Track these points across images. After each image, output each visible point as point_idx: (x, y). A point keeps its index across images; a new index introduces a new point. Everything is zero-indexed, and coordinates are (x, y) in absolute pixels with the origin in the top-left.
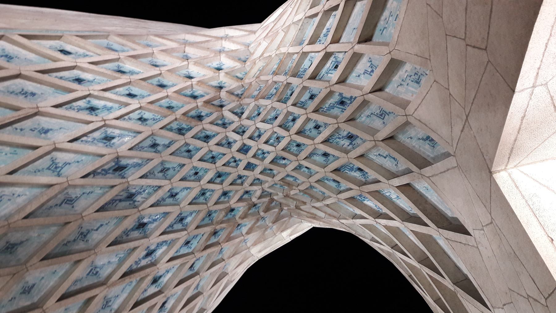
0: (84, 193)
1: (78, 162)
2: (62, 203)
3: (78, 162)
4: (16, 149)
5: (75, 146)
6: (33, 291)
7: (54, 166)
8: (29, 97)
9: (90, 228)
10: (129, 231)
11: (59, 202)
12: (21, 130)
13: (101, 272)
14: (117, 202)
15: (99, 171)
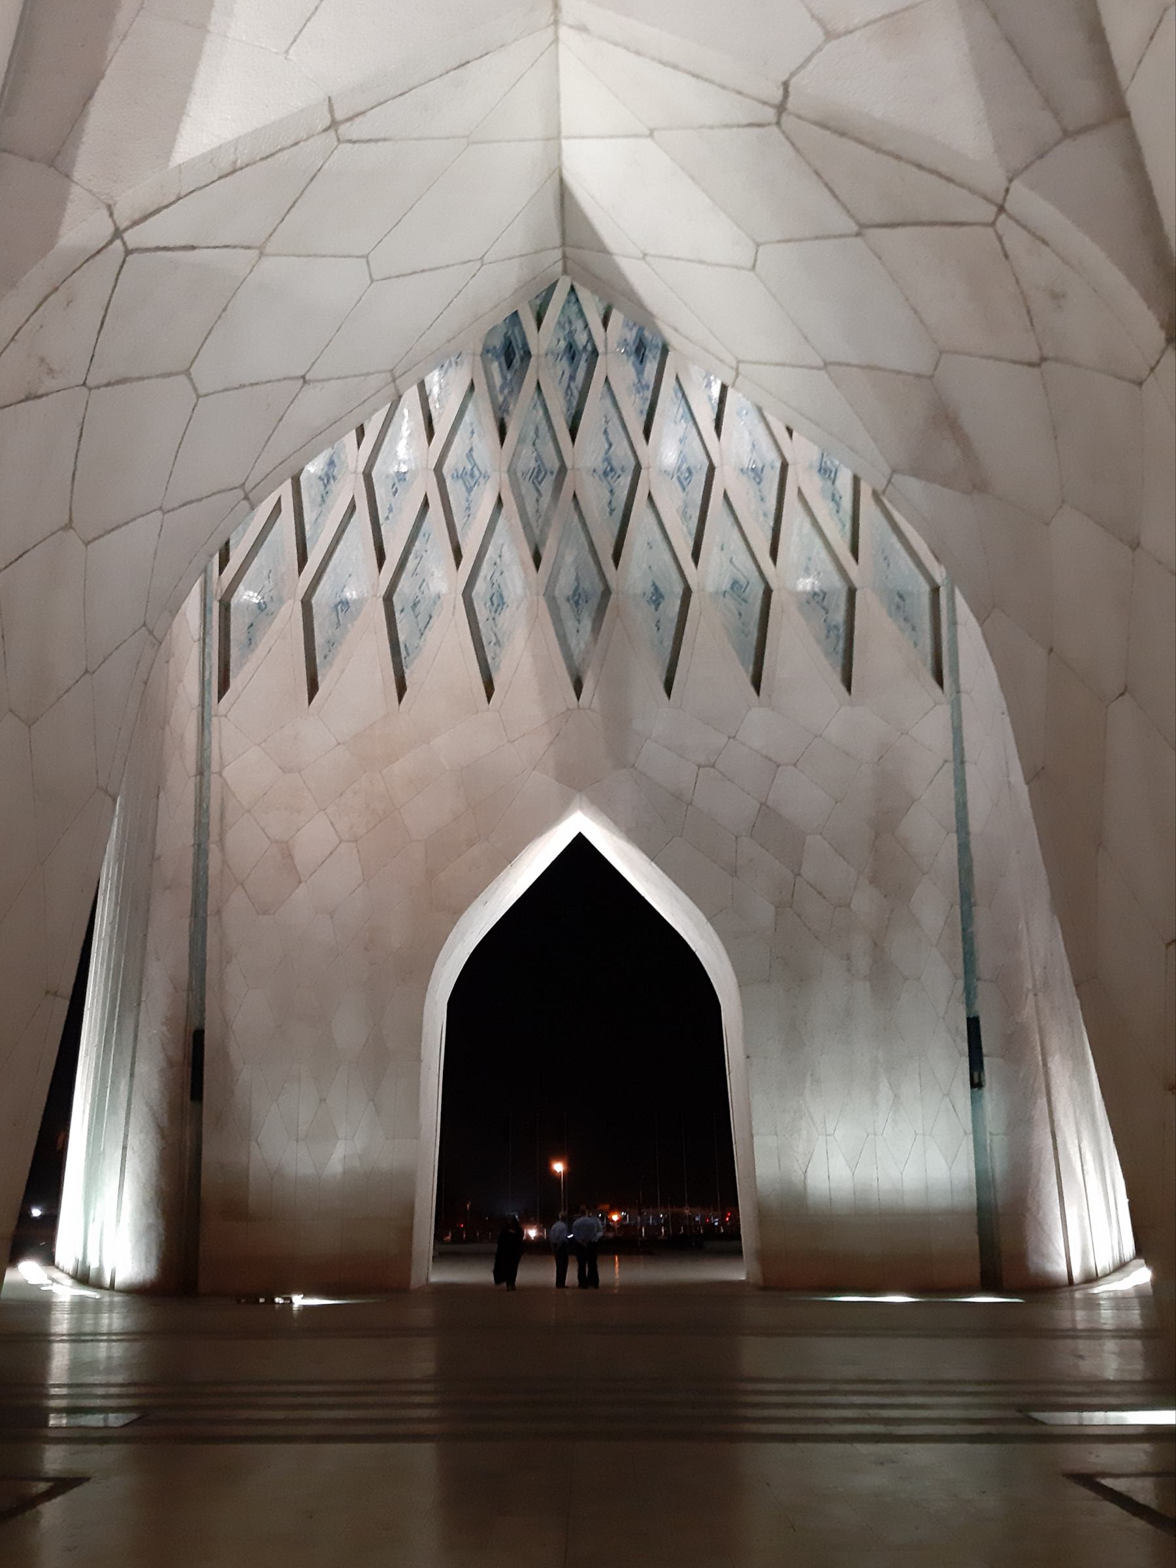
0: (534, 444)
1: (473, 432)
2: (538, 491)
3: (473, 432)
4: (421, 534)
5: (442, 429)
6: (662, 590)
7: (468, 477)
8: (335, 473)
9: (600, 459)
10: (639, 381)
11: (535, 495)
12: (390, 510)
13: (691, 462)
14: (573, 385)
15: (501, 399)
